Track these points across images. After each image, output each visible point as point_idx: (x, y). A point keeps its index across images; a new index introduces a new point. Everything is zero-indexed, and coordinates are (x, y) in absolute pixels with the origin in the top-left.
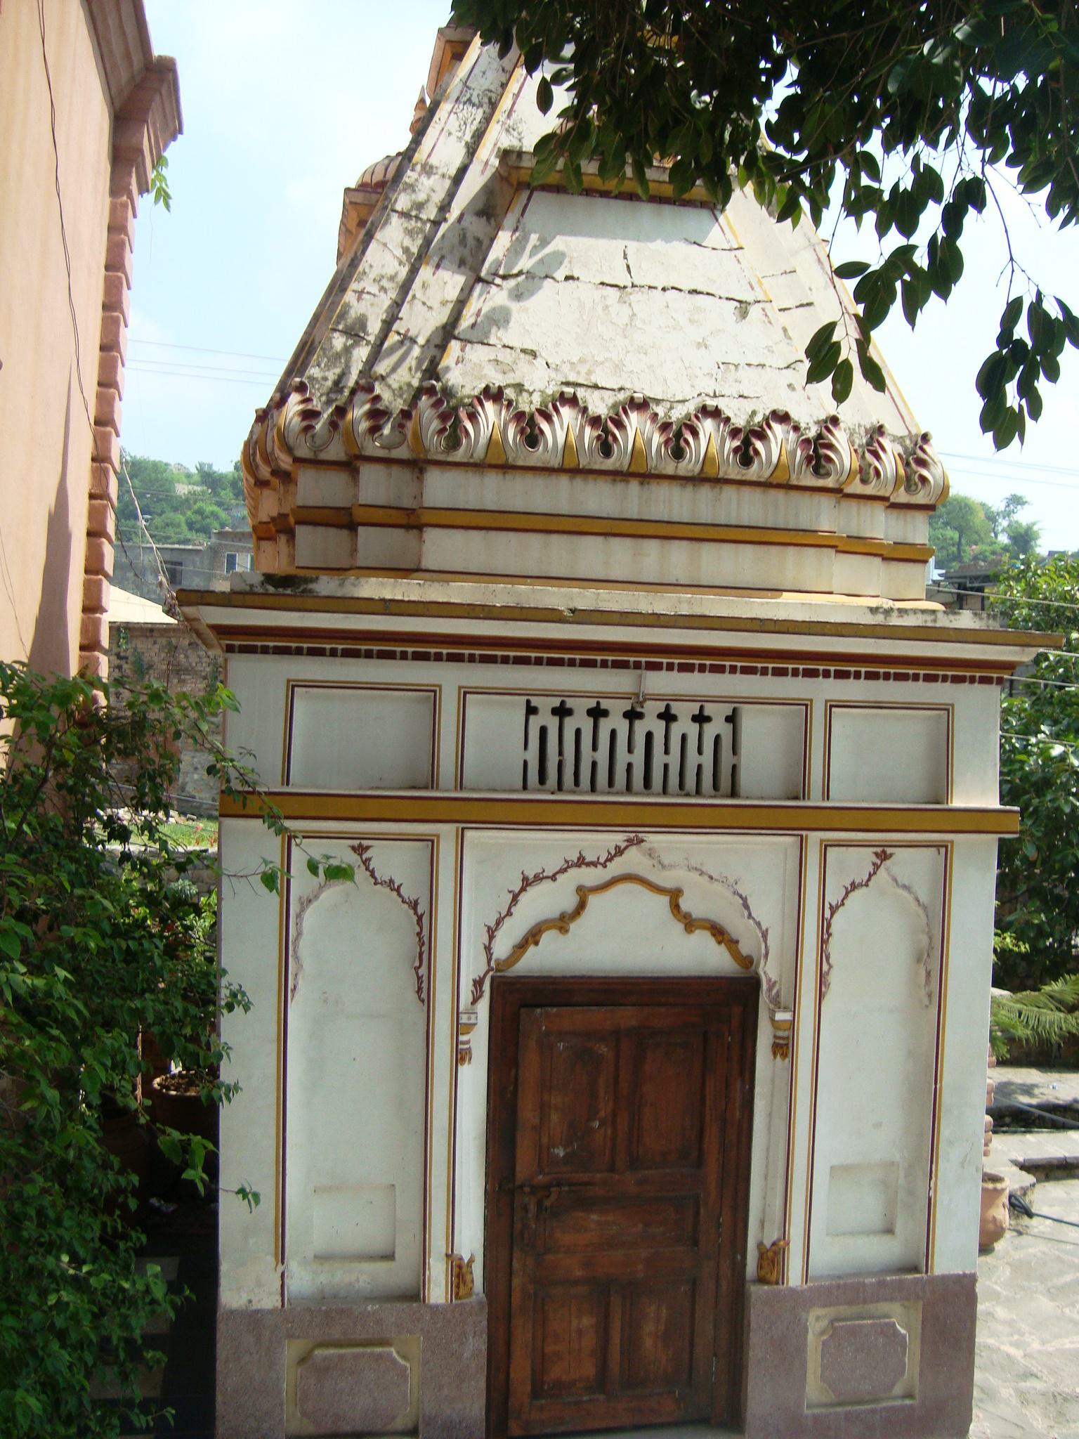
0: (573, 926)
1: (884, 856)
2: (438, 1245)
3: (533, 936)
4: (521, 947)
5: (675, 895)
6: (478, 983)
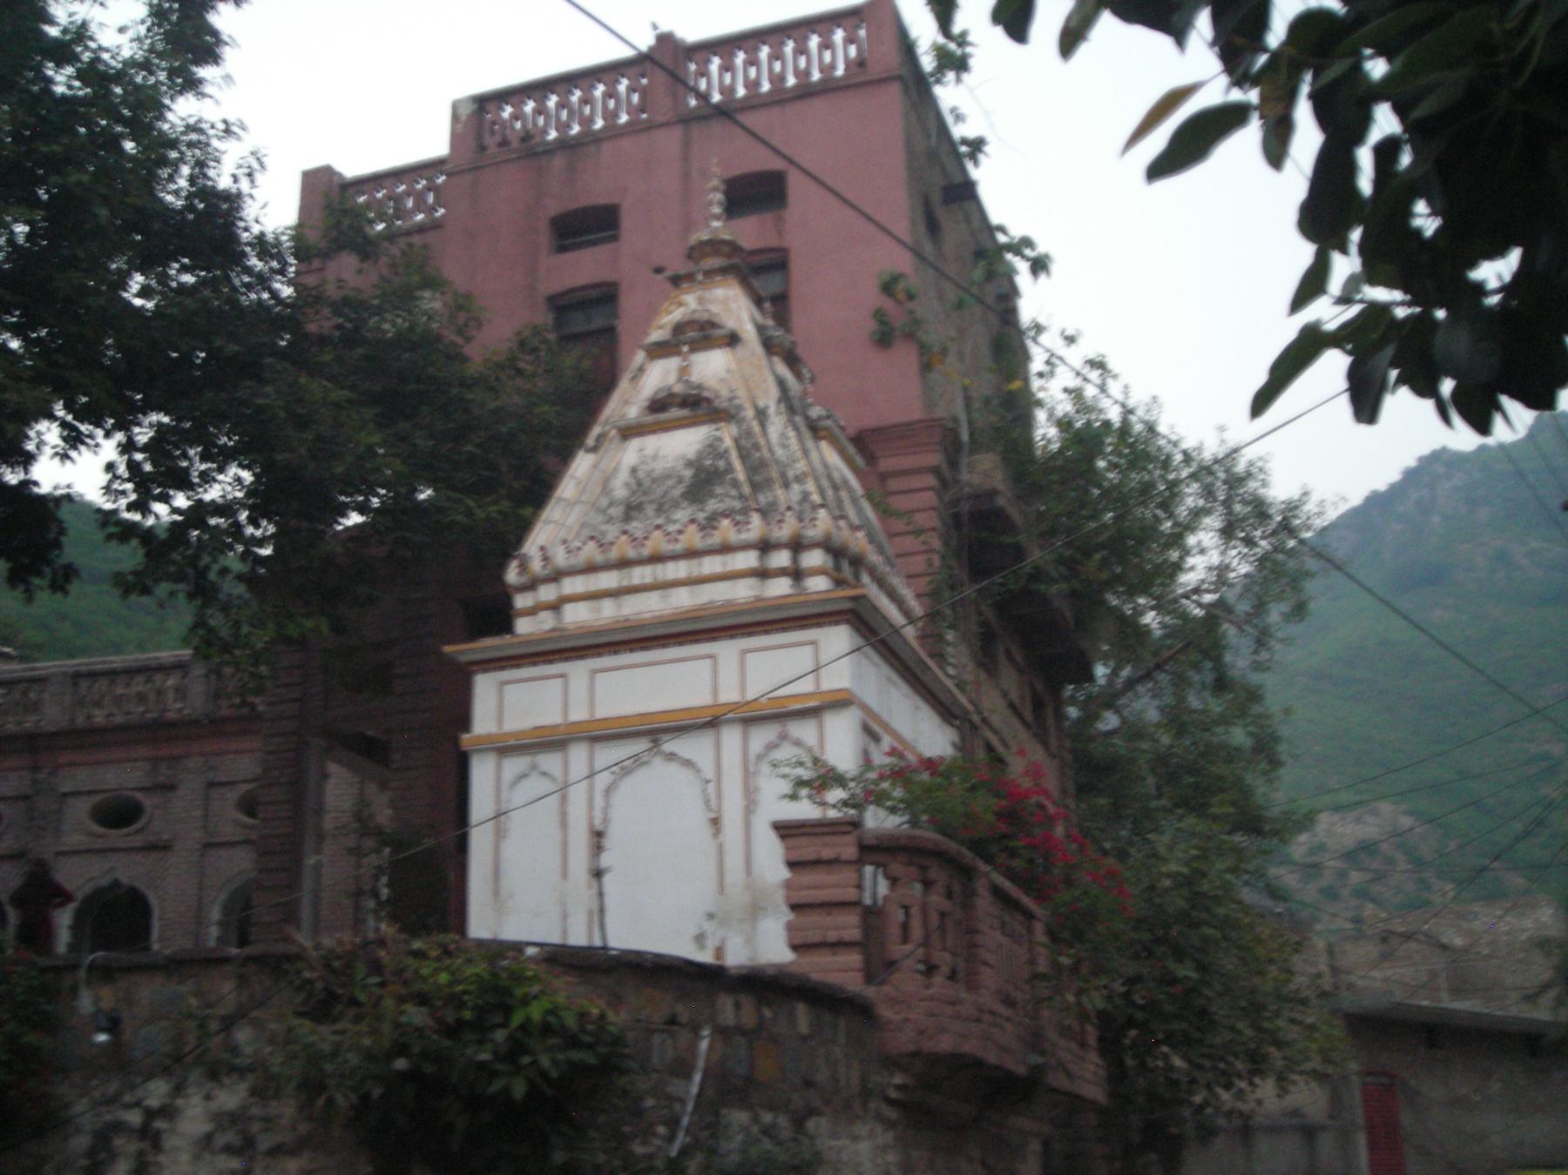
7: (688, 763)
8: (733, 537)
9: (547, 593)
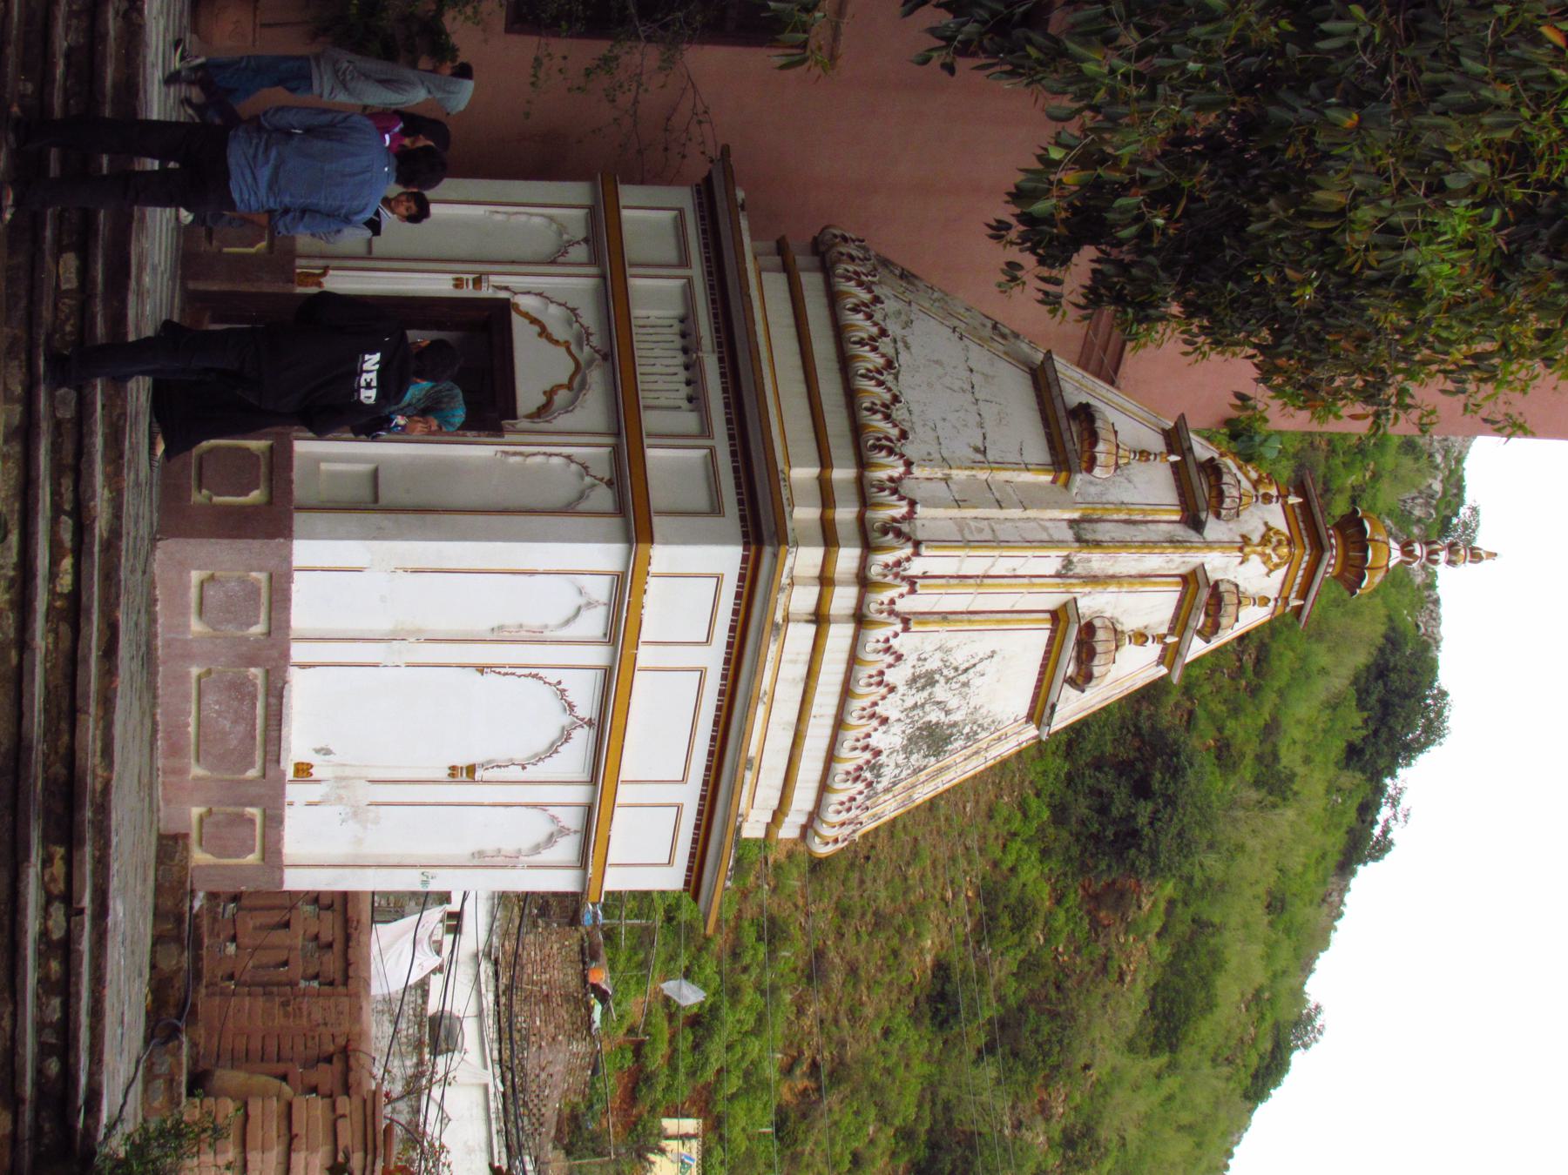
0: (543, 341)
1: (610, 483)
2: (336, 263)
3: (534, 321)
4: (526, 315)
5: (569, 387)
6: (506, 288)
7: (553, 749)
8: (834, 799)
9: (844, 599)
